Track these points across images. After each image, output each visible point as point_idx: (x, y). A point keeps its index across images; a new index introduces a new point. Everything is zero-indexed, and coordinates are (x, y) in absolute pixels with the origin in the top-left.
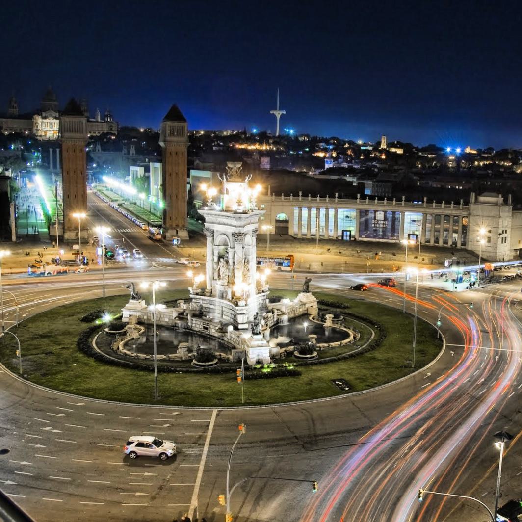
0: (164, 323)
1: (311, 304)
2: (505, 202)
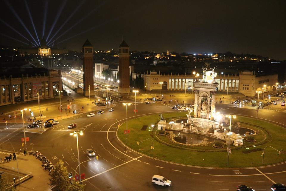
0: (177, 130)
2: (253, 74)
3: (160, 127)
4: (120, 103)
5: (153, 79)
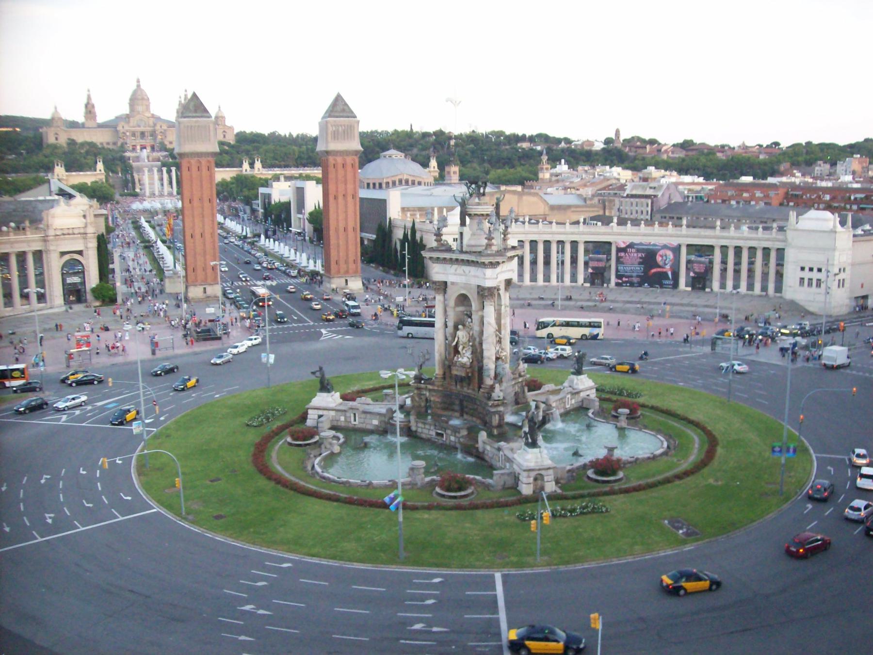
1: (588, 393)
3: (316, 417)
4: (313, 327)
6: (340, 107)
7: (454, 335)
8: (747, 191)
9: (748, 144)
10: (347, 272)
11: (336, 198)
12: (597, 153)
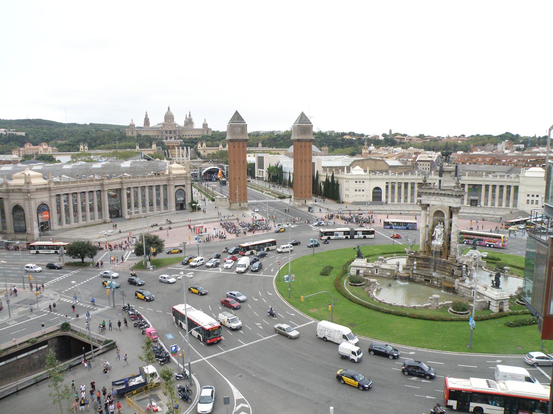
3: (356, 271)
5: (356, 182)
6: (303, 119)
7: (433, 231)
8: (474, 158)
9: (450, 136)
10: (306, 197)
11: (301, 161)
12: (381, 141)
